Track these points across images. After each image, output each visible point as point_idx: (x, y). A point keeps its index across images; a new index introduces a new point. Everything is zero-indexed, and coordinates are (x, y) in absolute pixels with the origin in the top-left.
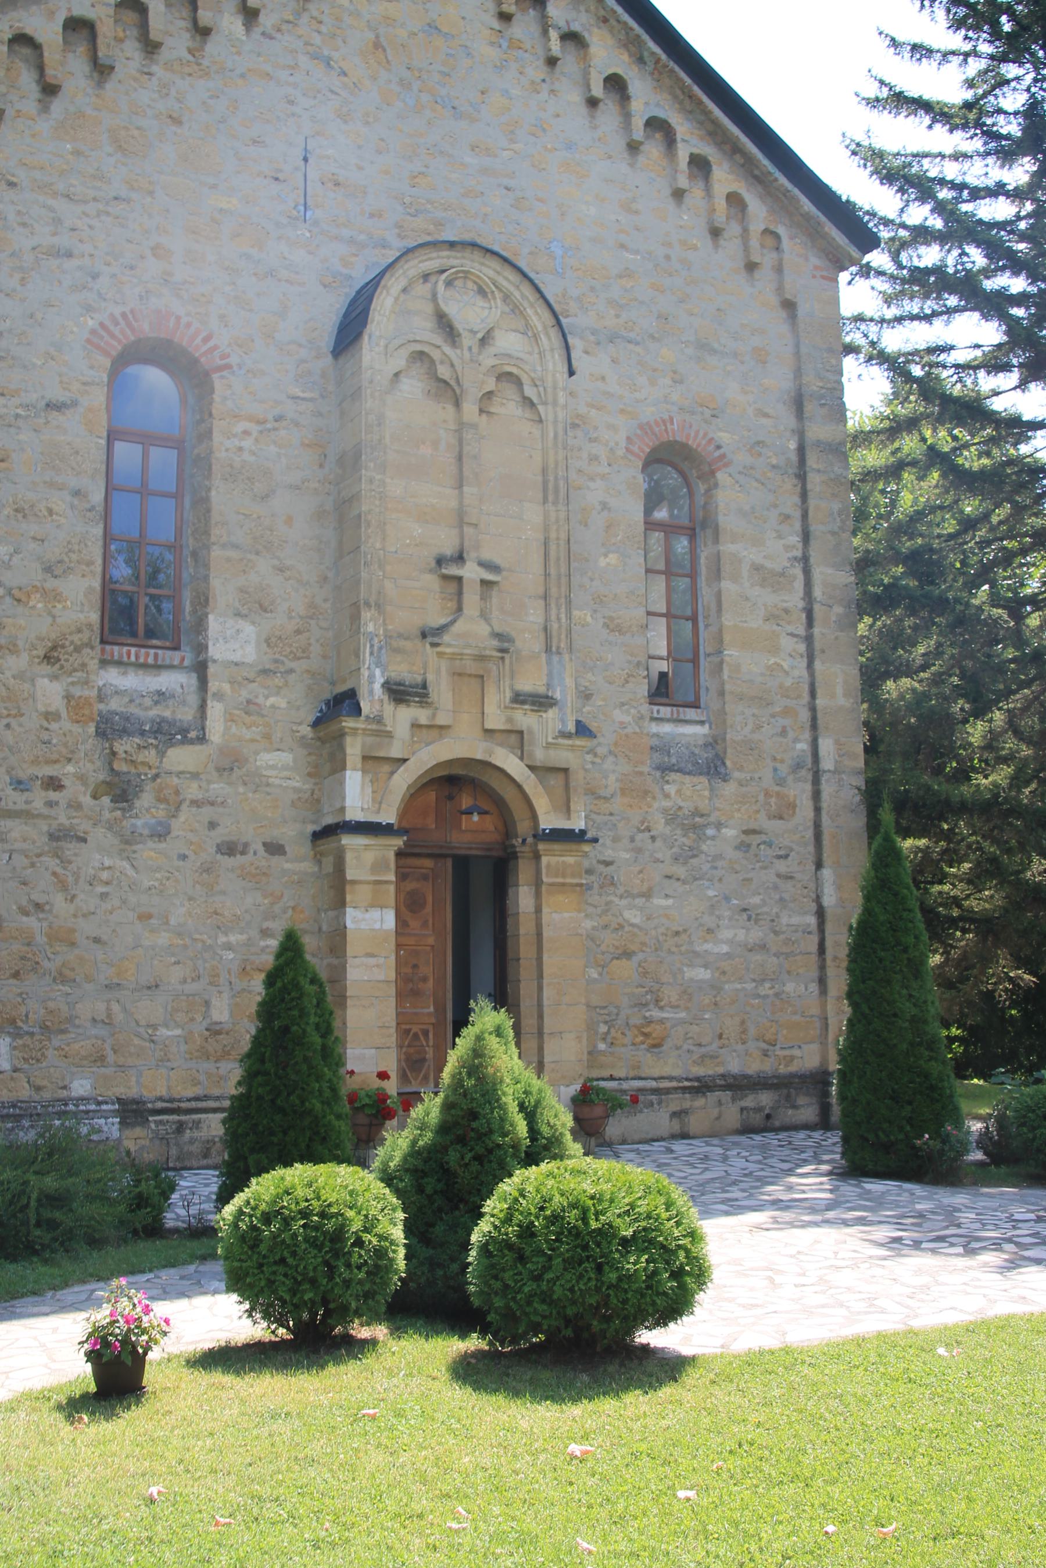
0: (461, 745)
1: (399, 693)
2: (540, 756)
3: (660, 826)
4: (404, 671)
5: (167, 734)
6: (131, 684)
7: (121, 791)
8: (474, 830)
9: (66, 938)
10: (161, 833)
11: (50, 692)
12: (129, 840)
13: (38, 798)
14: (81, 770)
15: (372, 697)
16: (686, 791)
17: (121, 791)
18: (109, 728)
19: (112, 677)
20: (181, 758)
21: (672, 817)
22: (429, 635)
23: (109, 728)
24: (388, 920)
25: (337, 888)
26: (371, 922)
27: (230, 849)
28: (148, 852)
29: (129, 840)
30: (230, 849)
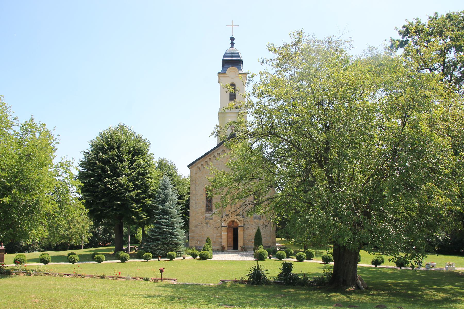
0: (233, 219)
1: (227, 215)
2: (239, 220)
3: (254, 224)
4: (227, 214)
5: (210, 219)
6: (208, 215)
7: (207, 223)
8: (235, 226)
9: (203, 234)
10: (210, 227)
11: (201, 216)
12: (207, 227)
13: (201, 224)
14: (204, 222)
15: (224, 215)
16: (257, 221)
17: (207, 223)
18: (206, 219)
19: (207, 215)
20: (211, 221)
21: (255, 223)
22: (230, 210)
23: (206, 219)
24: (226, 233)
25: (222, 231)
26: (225, 233)
27: (215, 227)
28: (209, 228)
29: (207, 227)
30: (215, 227)
